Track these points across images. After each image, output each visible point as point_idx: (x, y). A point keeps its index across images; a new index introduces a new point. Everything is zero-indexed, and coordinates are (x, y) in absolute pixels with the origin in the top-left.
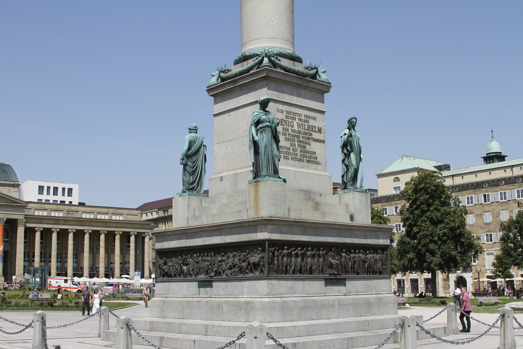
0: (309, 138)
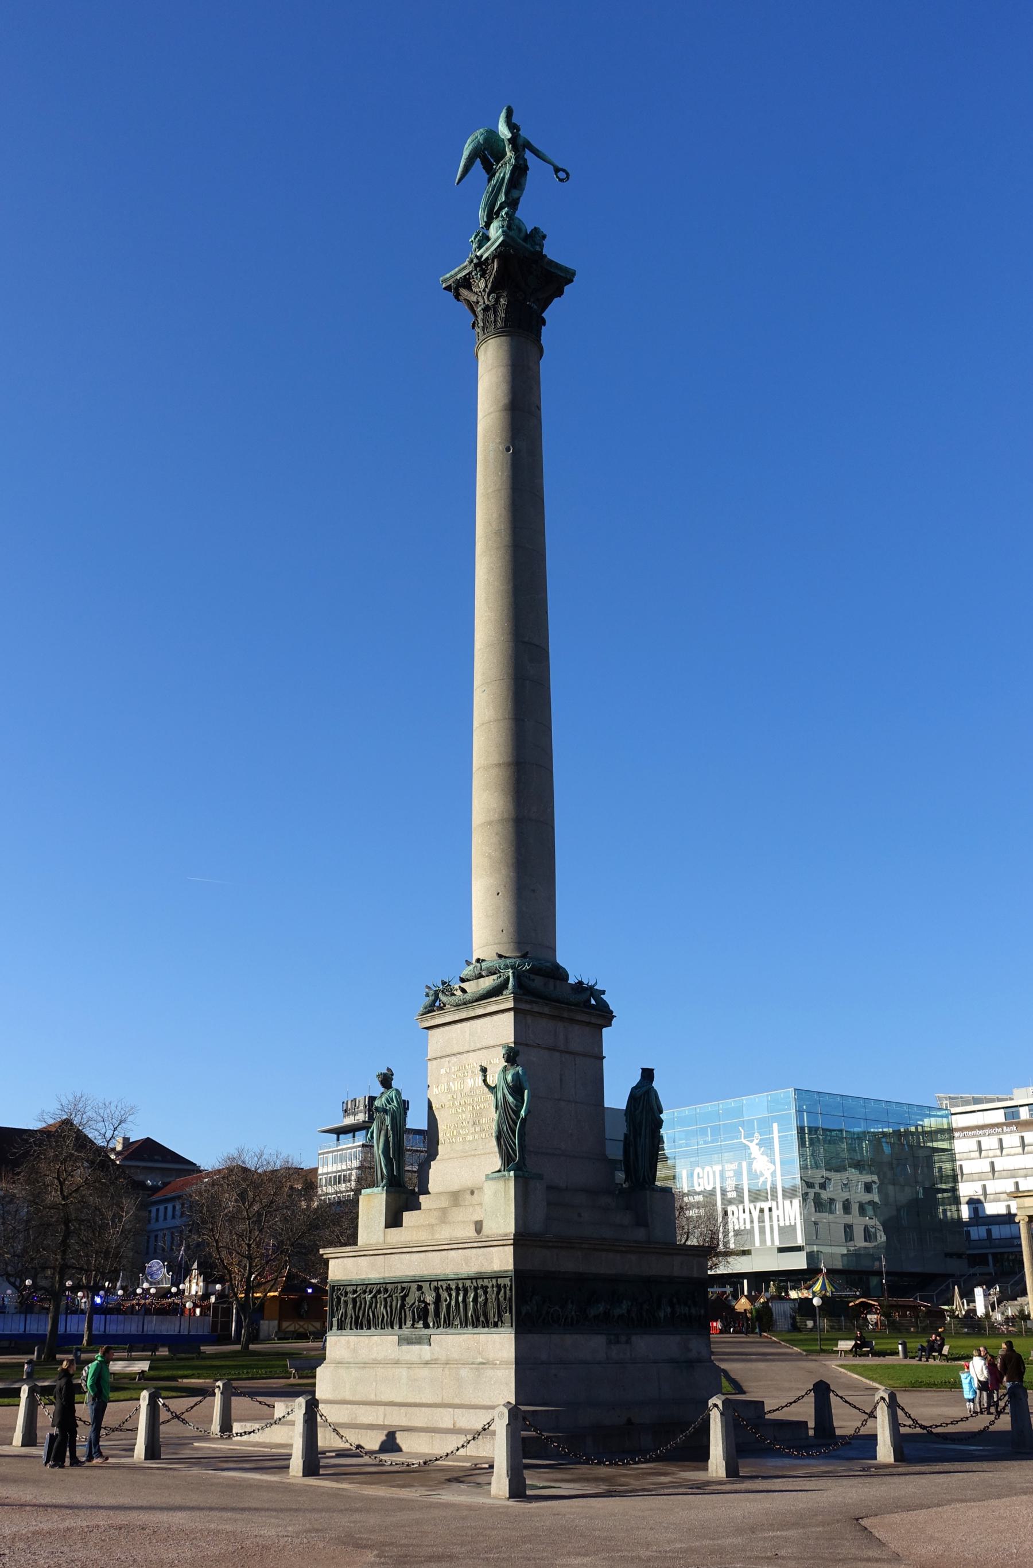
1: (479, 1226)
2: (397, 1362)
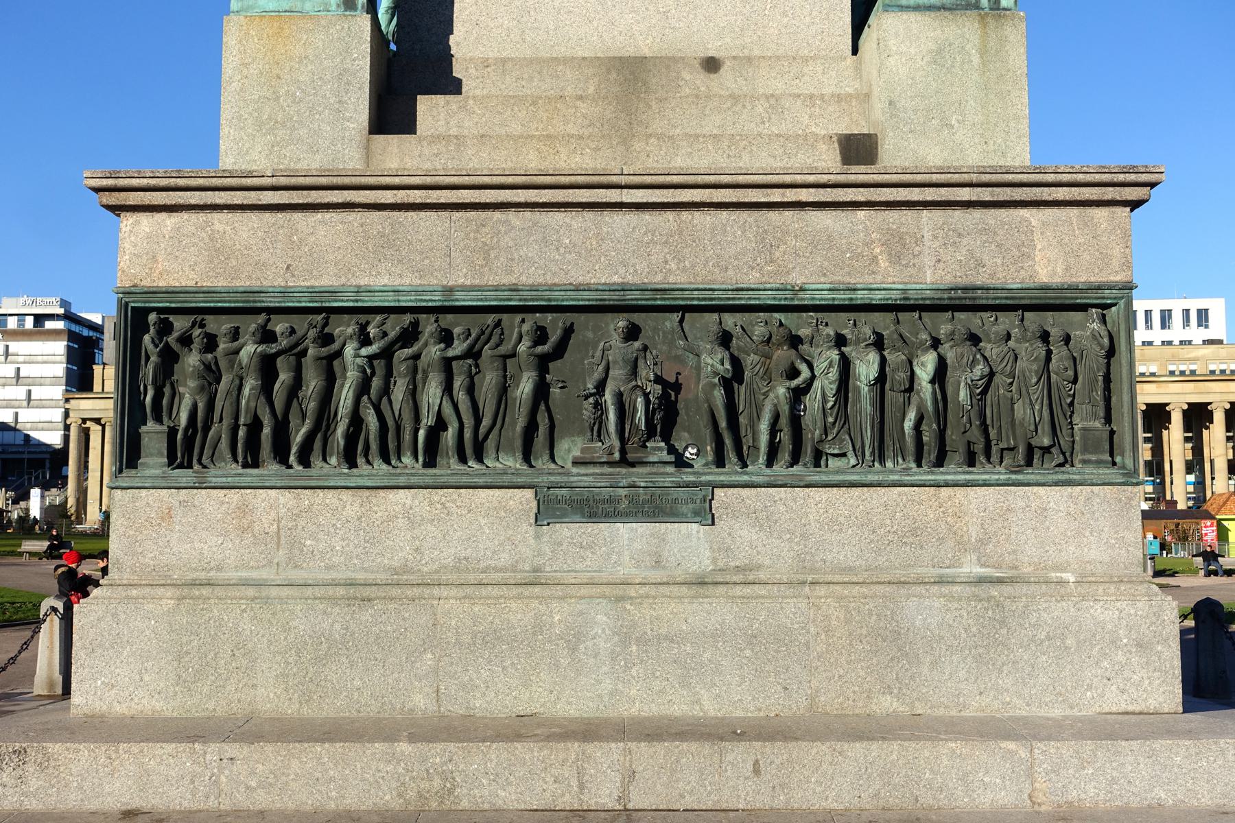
2: (535, 580)
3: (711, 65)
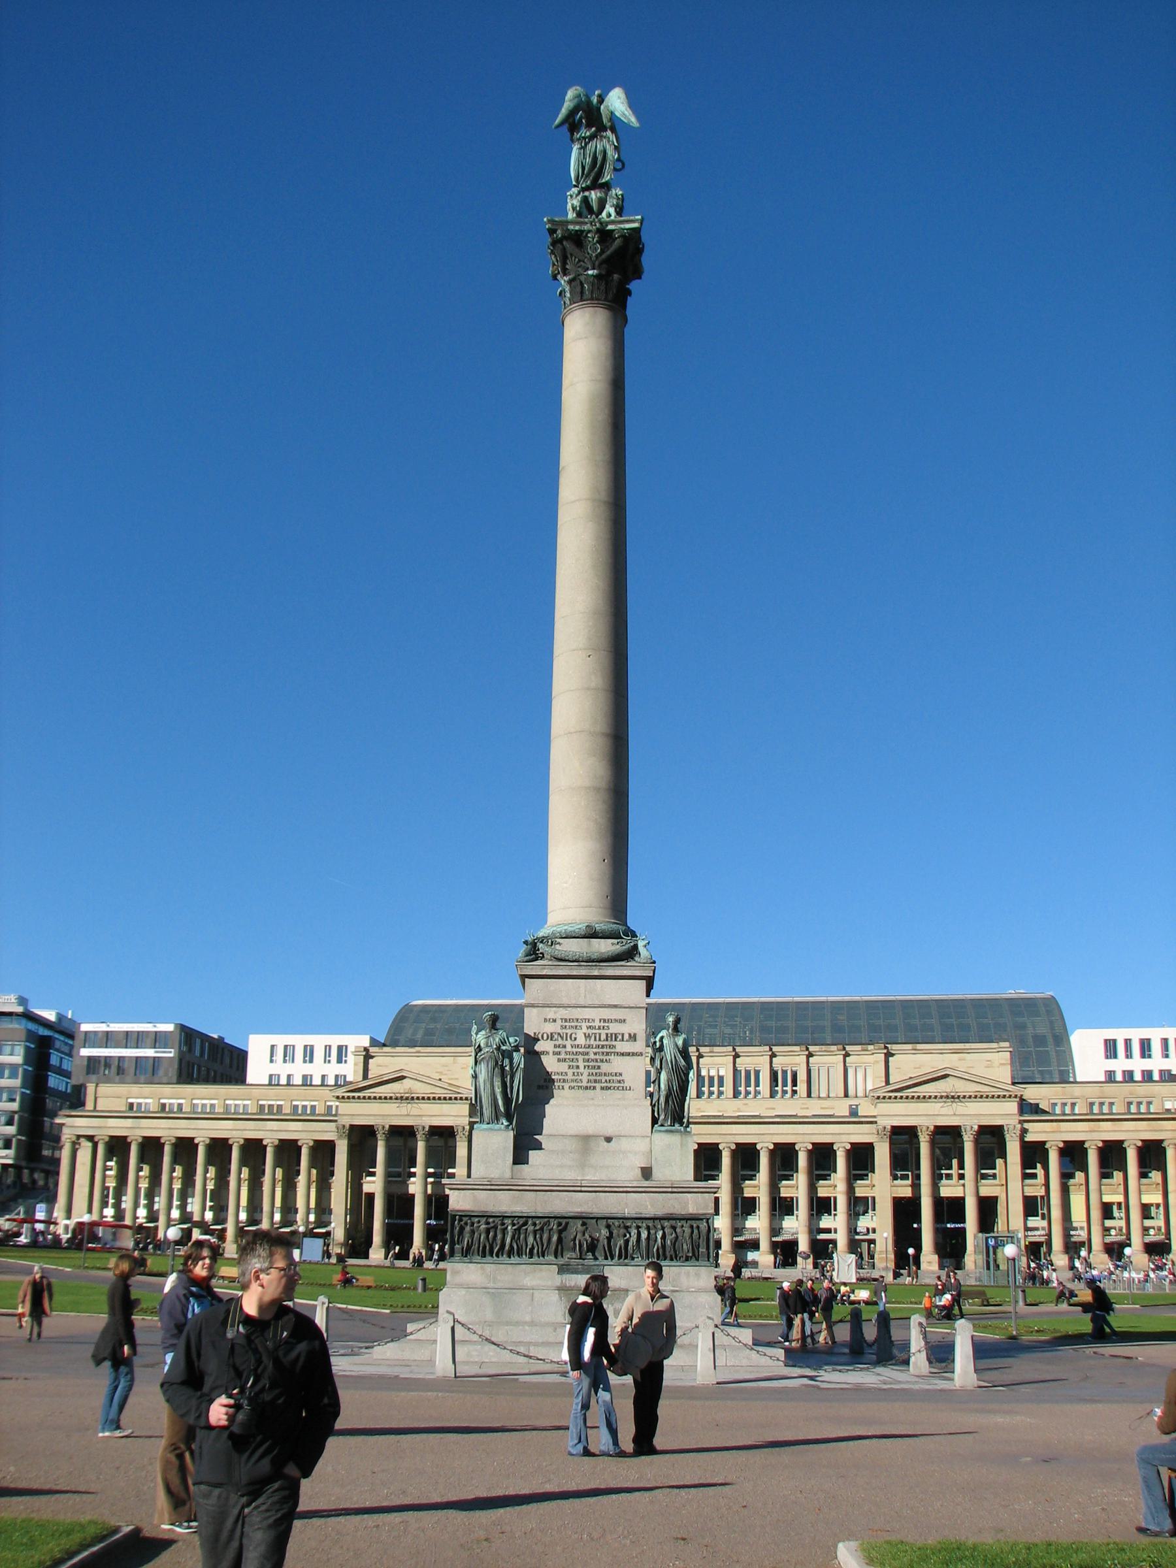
0: (607, 1054)
1: (647, 1173)
3: (609, 1140)
